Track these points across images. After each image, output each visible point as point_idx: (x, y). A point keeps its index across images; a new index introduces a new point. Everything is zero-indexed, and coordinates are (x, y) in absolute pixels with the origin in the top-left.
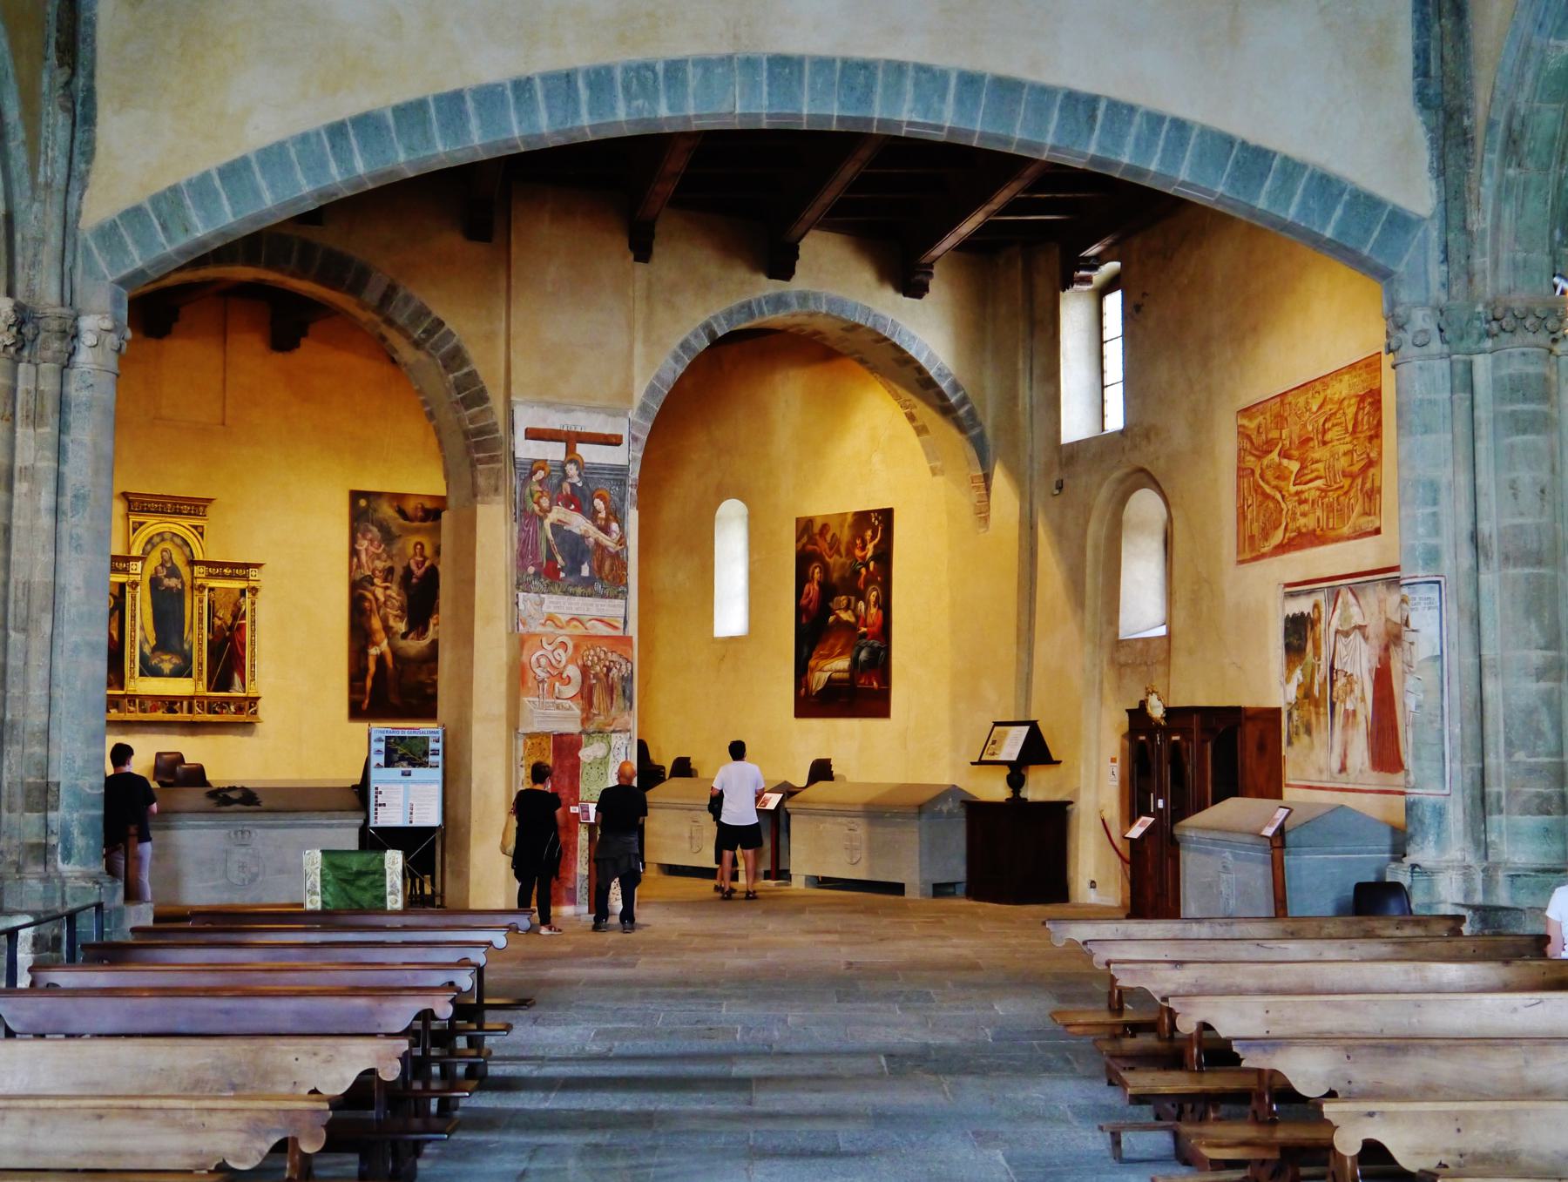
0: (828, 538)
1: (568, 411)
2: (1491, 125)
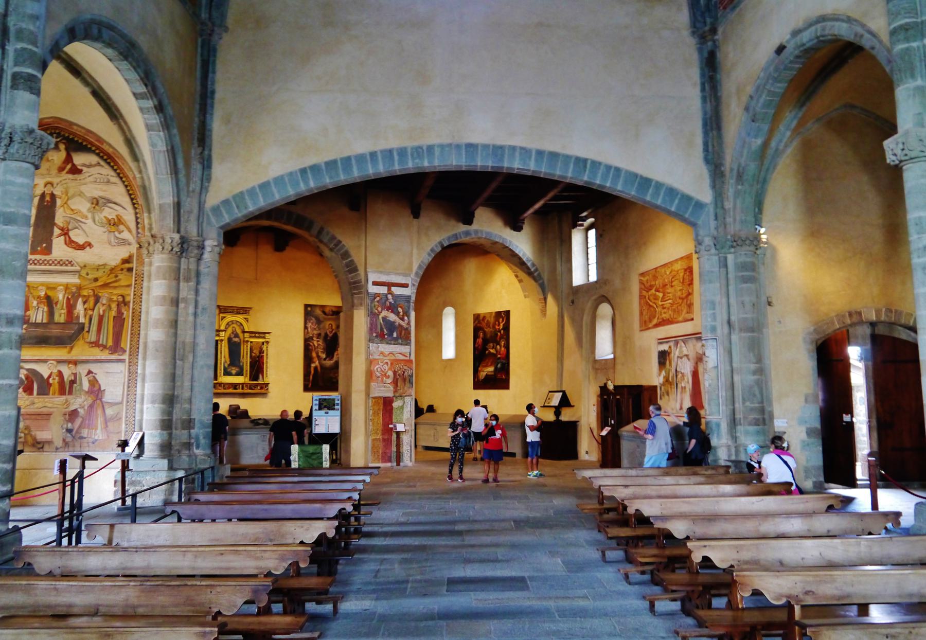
2: (732, 170)
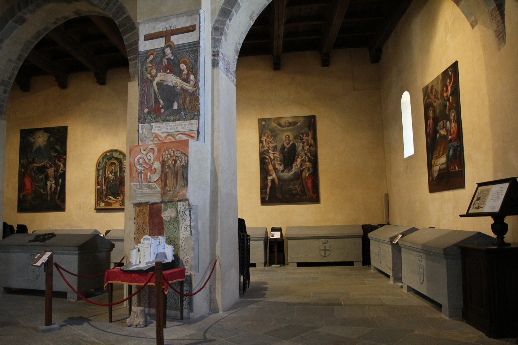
0: (434, 93)
1: (167, 18)
